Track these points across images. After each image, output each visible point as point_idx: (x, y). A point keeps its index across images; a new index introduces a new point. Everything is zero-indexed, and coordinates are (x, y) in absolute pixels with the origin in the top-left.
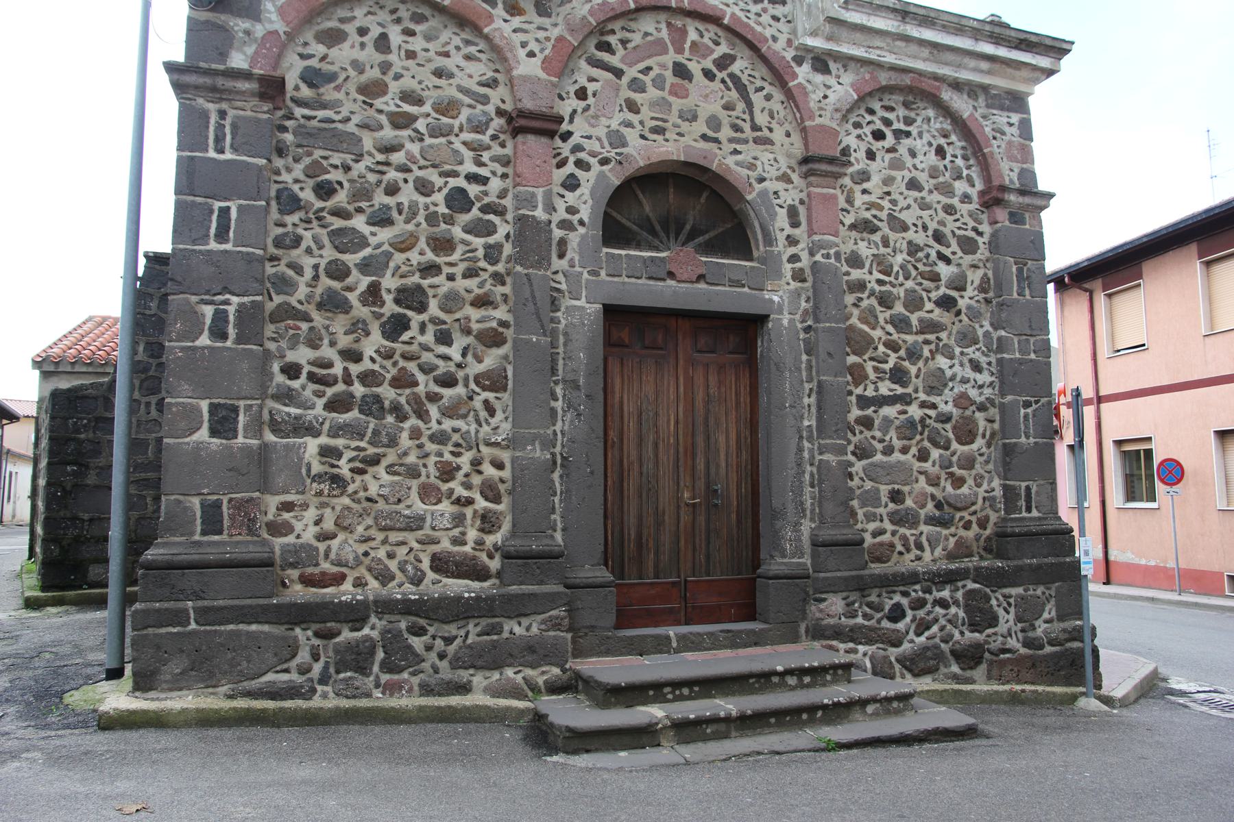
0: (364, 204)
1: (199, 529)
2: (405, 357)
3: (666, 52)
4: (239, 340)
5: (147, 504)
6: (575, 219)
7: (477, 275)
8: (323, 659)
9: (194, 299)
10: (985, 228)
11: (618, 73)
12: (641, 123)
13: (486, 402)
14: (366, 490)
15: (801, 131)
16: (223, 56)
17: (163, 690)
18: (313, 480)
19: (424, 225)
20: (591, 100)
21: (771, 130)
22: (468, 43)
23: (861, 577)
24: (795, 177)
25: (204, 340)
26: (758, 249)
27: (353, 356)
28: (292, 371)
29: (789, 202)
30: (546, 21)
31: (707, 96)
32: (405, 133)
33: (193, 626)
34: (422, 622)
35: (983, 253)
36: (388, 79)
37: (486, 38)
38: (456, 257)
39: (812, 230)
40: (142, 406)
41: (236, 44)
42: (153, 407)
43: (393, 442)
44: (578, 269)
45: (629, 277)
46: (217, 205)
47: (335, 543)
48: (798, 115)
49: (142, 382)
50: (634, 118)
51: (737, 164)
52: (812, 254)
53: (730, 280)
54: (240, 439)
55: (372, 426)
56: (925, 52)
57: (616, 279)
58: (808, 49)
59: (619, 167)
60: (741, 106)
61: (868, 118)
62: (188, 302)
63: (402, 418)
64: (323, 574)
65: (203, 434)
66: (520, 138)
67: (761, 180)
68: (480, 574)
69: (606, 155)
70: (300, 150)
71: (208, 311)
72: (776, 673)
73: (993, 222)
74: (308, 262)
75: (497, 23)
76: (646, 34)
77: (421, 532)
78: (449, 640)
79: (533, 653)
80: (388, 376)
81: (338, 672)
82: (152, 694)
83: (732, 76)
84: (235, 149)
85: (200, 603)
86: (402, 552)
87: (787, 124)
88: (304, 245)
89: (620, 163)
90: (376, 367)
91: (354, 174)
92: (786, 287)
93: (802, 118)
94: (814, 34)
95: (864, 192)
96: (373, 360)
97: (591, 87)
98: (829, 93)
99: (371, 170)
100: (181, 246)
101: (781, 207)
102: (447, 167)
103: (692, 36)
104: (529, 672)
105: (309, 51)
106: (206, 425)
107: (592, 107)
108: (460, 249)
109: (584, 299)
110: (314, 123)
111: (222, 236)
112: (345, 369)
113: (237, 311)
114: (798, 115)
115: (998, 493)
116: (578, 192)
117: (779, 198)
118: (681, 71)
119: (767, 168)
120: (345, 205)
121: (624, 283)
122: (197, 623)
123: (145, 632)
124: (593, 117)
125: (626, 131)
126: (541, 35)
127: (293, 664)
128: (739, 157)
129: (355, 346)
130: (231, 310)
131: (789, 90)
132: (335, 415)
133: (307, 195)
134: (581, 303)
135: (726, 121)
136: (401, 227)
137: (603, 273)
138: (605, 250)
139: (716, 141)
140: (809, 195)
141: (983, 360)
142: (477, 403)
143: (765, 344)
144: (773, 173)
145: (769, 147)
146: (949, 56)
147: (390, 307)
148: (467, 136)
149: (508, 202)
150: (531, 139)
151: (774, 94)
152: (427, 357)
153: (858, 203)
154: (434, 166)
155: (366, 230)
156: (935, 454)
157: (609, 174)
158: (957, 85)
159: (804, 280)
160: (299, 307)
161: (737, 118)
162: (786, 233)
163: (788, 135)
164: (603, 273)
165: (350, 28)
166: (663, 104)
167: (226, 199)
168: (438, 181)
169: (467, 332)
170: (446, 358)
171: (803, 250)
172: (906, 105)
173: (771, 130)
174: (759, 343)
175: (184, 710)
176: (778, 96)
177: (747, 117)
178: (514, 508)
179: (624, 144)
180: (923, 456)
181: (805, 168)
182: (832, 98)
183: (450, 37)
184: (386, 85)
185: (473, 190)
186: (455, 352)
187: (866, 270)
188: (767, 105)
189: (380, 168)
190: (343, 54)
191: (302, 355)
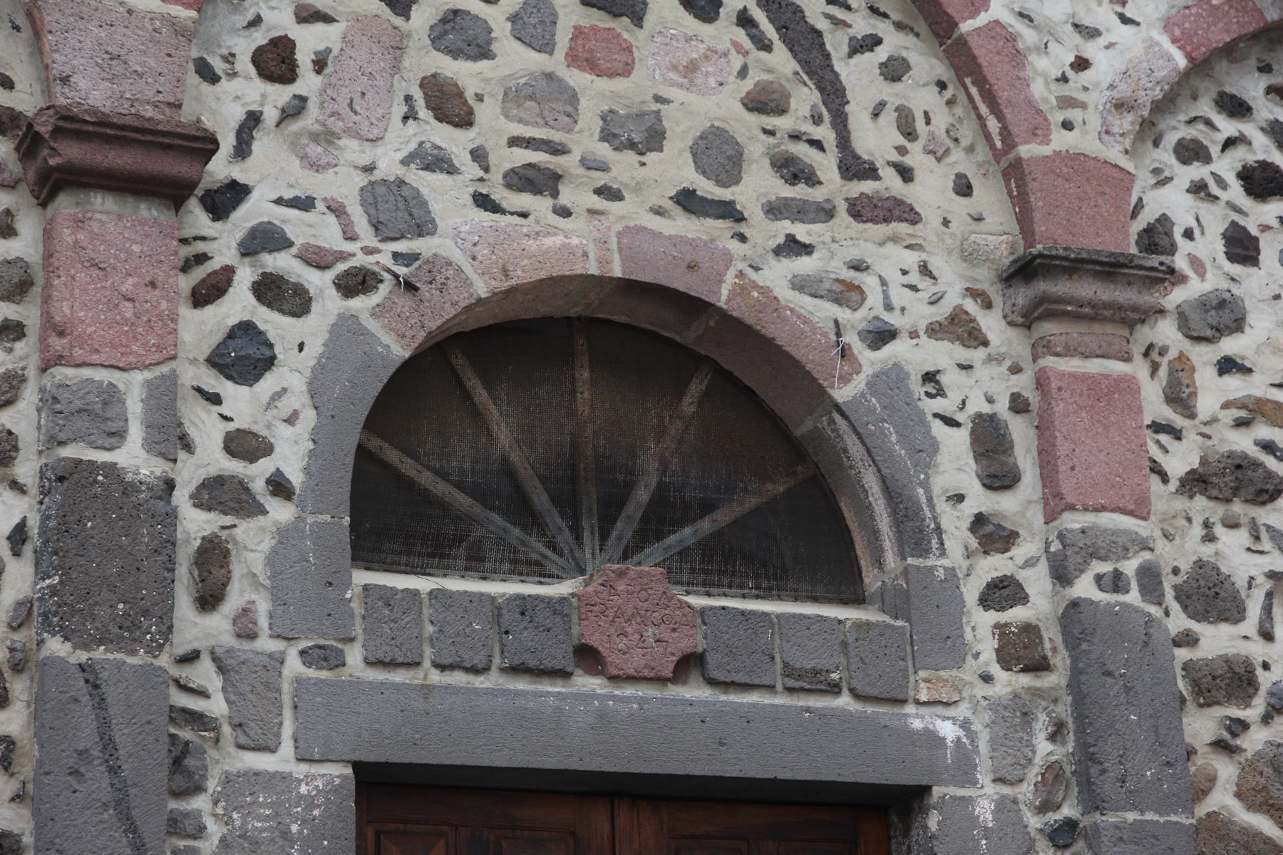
6: (257, 473)
12: (479, 155)
15: (1006, 175)
20: (308, 83)
21: (906, 174)
24: (991, 324)
26: (879, 563)
29: (978, 405)
31: (692, 68)
39: (1059, 496)
44: (266, 644)
45: (442, 667)
48: (993, 125)
50: (455, 142)
51: (799, 284)
52: (1062, 576)
53: (789, 671)
57: (399, 677)
59: (404, 303)
60: (805, 98)
61: (1228, 127)
66: (65, 204)
67: (881, 336)
69: (361, 260)
87: (957, 155)
89: (410, 287)
92: (981, 690)
93: (1006, 133)
95: (1227, 366)
97: (308, 40)
98: (1091, 50)
101: (951, 422)
107: (313, 109)
109: (287, 748)
114: (993, 125)
116: (268, 384)
117: (941, 393)
119: (899, 296)
121: (427, 690)
124: (315, 137)
125: (427, 183)
128: (804, 265)
131: (962, 43)
134: (281, 760)
135: (757, 150)
137: (354, 656)
138: (362, 577)
139: (728, 211)
140: (1041, 382)
144: (919, 312)
145: (902, 228)
150: (103, 205)
151: (913, 57)
153: (1207, 404)
157: (372, 325)
159: (1039, 666)
161: (795, 137)
162: (969, 508)
163: (964, 188)
164: (354, 656)
171: (1030, 563)
173: (906, 174)
177: (825, 133)
179: (423, 226)
181: (1023, 295)
182: (1105, 66)
187: (1250, 625)
188: (892, 93)
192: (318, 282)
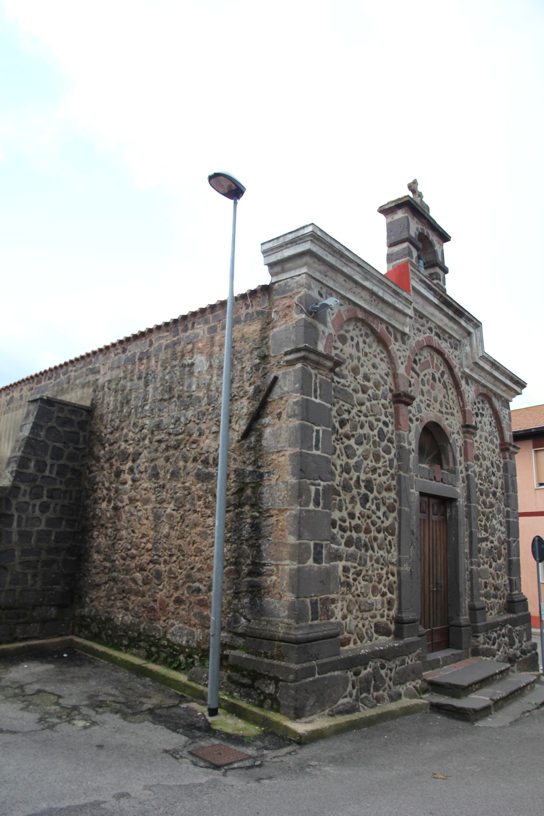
0: (354, 433)
1: (310, 617)
2: (369, 517)
3: (429, 368)
4: (324, 508)
5: (27, 580)
7: (387, 475)
8: (356, 687)
9: (308, 482)
10: (502, 461)
11: (418, 375)
13: (390, 541)
14: (357, 589)
15: (462, 411)
16: (316, 343)
17: (307, 717)
18: (342, 586)
19: (372, 447)
22: (382, 352)
23: (486, 625)
24: (460, 432)
25: (311, 507)
26: (448, 464)
27: (352, 516)
28: (333, 524)
30: (403, 346)
32: (366, 396)
33: (317, 676)
34: (384, 661)
35: (501, 473)
36: (360, 365)
37: (389, 352)
38: (380, 465)
40: (30, 507)
41: (320, 338)
42: (37, 508)
43: (365, 565)
45: (421, 477)
46: (316, 428)
47: (348, 620)
48: (461, 404)
49: (32, 489)
50: (423, 399)
52: (467, 470)
54: (324, 564)
55: (359, 555)
56: (492, 380)
58: (464, 373)
62: (306, 482)
63: (367, 550)
64: (345, 638)
65: (310, 562)
67: (453, 433)
68: (387, 633)
70: (335, 400)
71: (313, 488)
72: (496, 674)
73: (505, 458)
74: (338, 463)
75: (393, 346)
76: (425, 358)
77: (372, 612)
78: (391, 670)
79: (415, 673)
80: (364, 527)
81: (361, 694)
82: (304, 720)
83: (444, 381)
84: (321, 398)
85: (320, 661)
86: (367, 622)
88: (337, 454)
90: (359, 522)
91: (351, 415)
94: (468, 367)
96: (359, 518)
99: (357, 415)
100: (304, 451)
102: (378, 417)
103: (435, 361)
104: (414, 683)
105: (336, 346)
106: (312, 556)
108: (382, 460)
110: (340, 386)
111: (317, 447)
112: (350, 523)
113: (323, 490)
115: (507, 582)
118: (434, 378)
120: (349, 432)
122: (319, 674)
123: (301, 682)
125: (421, 404)
126: (404, 354)
127: (347, 692)
129: (353, 510)
130: (320, 488)
132: (347, 548)
133: (337, 425)
135: (444, 403)
136: (365, 447)
139: (441, 412)
141: (503, 521)
142: (387, 542)
143: (454, 512)
144: (455, 431)
146: (497, 383)
147: (363, 491)
148: (383, 401)
149: (394, 437)
152: (374, 517)
154: (374, 415)
155: (355, 447)
156: (494, 564)
158: (495, 394)
160: (337, 488)
165: (348, 336)
166: (429, 392)
167: (319, 425)
168: (375, 423)
169: (384, 504)
170: (379, 518)
172: (483, 402)
174: (448, 511)
175: (331, 726)
176: (455, 394)
178: (399, 597)
180: (490, 566)
181: (465, 429)
183: (376, 348)
184: (359, 369)
185: (385, 429)
186: (380, 514)
189: (359, 414)
190: (348, 349)
191: (336, 515)
192: (414, 419)
